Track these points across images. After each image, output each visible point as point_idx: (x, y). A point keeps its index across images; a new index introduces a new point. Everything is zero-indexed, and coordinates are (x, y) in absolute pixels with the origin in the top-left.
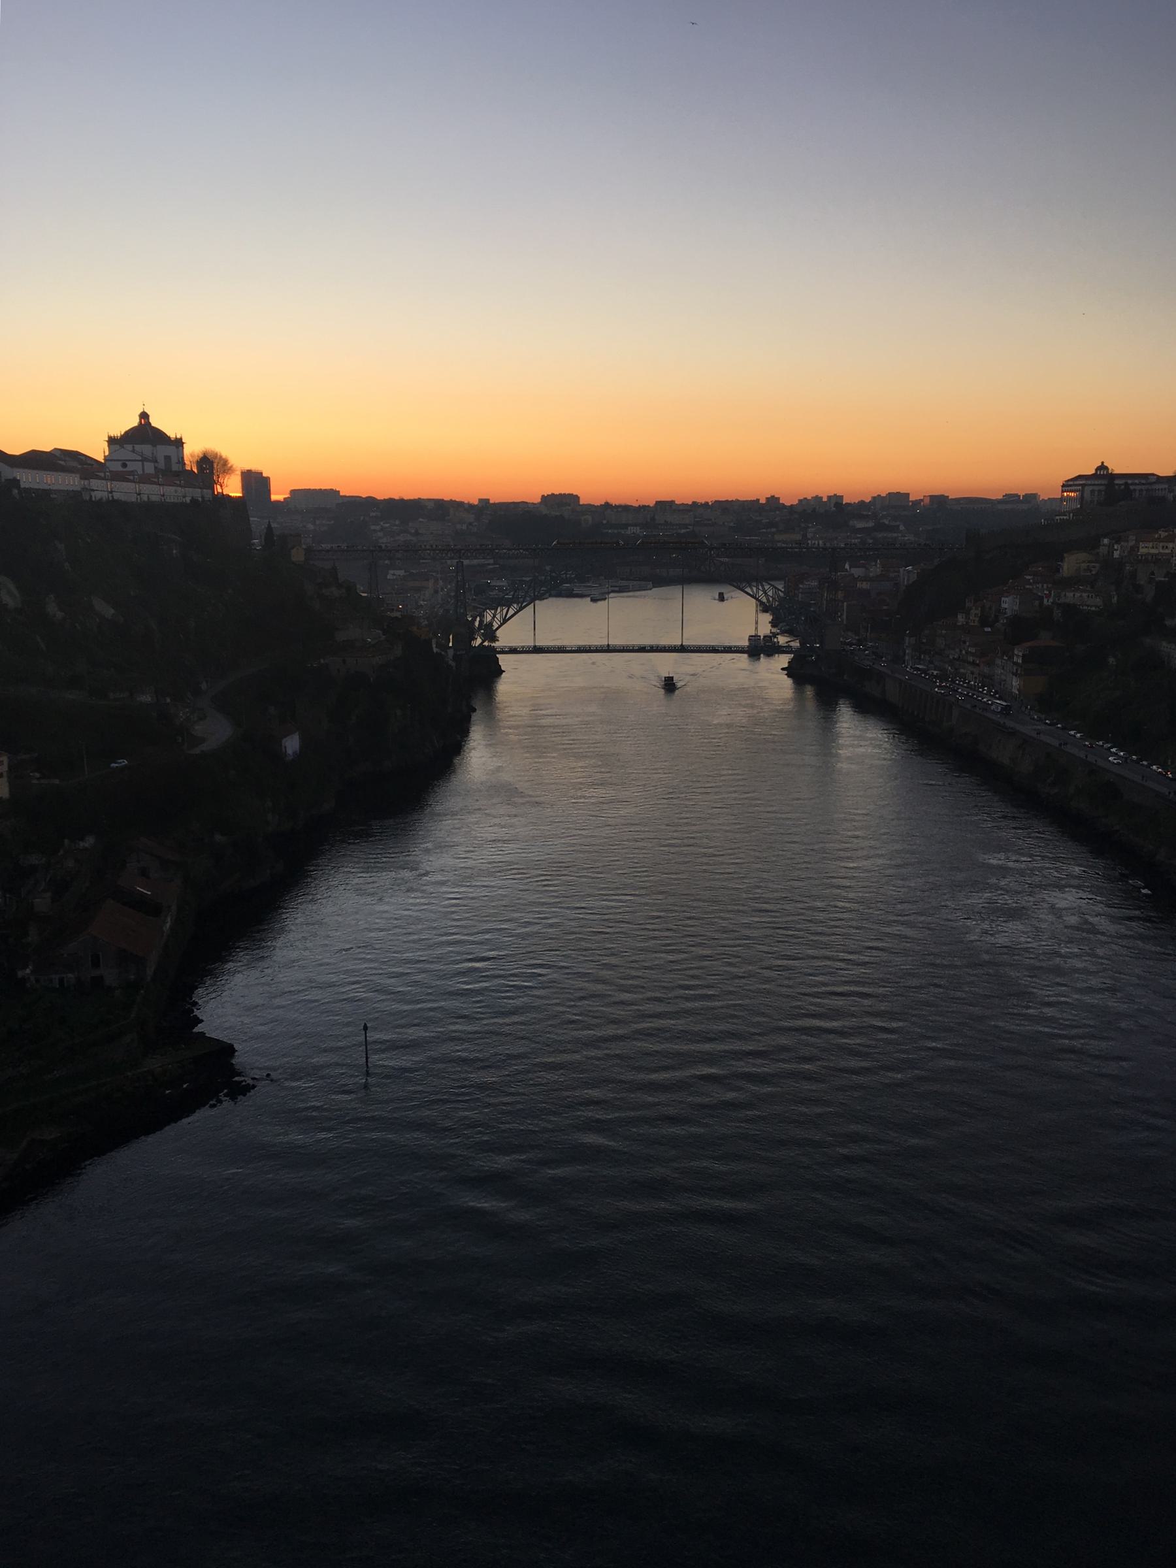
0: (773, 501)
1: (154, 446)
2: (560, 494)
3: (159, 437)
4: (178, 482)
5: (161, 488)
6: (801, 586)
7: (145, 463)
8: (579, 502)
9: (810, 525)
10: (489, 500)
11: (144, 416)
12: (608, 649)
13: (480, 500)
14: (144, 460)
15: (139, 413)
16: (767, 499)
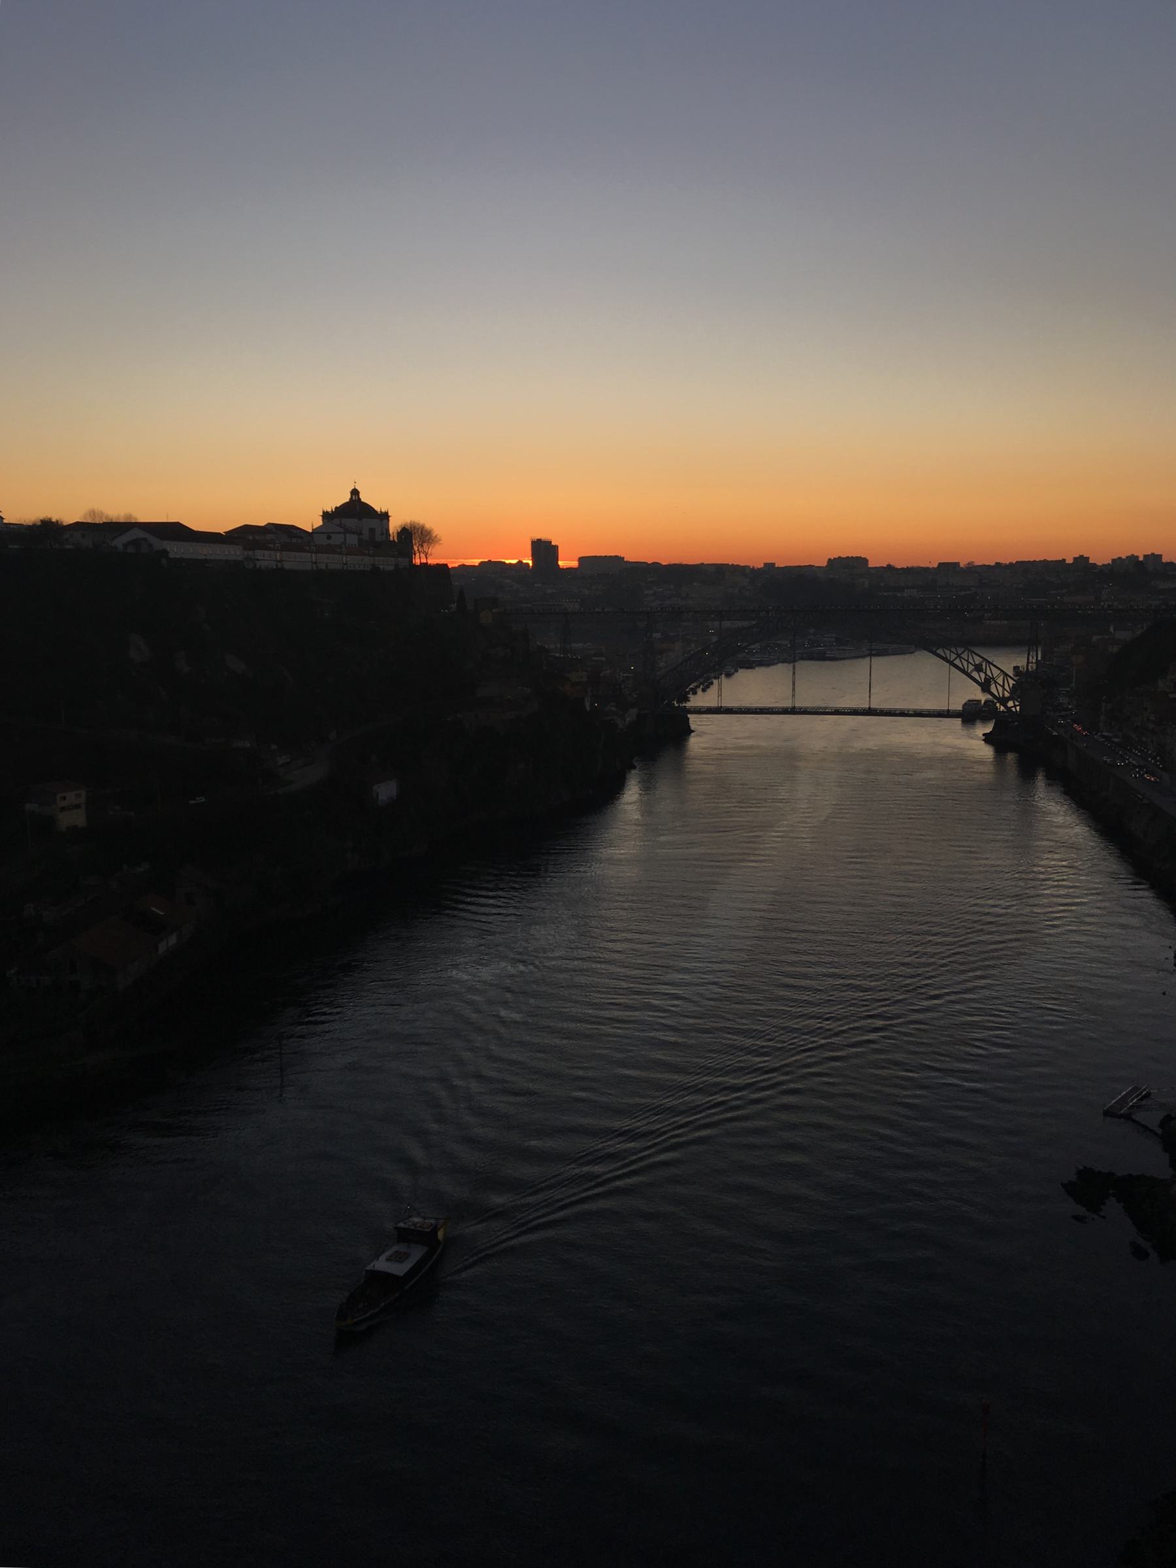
0: (1082, 561)
1: (360, 519)
2: (848, 557)
3: (367, 511)
4: (367, 552)
5: (344, 558)
6: (1056, 649)
7: (348, 535)
8: (867, 564)
9: (1106, 586)
10: (774, 564)
11: (355, 492)
12: (792, 711)
13: (766, 564)
14: (347, 531)
15: (351, 490)
16: (1075, 559)
